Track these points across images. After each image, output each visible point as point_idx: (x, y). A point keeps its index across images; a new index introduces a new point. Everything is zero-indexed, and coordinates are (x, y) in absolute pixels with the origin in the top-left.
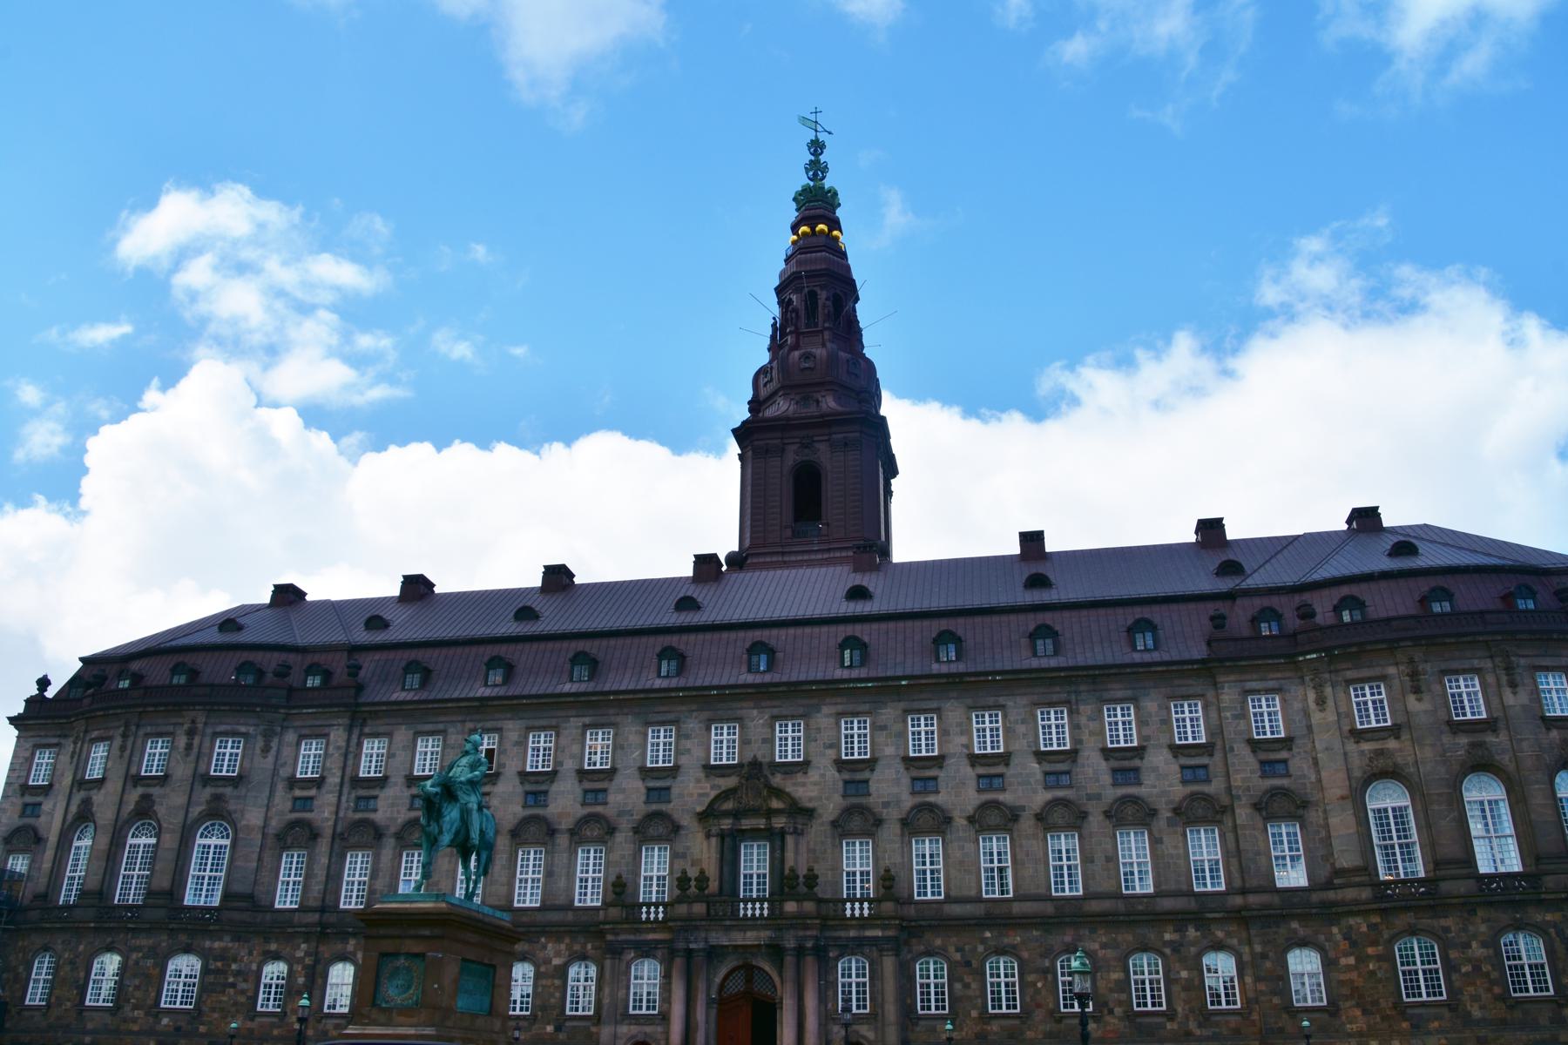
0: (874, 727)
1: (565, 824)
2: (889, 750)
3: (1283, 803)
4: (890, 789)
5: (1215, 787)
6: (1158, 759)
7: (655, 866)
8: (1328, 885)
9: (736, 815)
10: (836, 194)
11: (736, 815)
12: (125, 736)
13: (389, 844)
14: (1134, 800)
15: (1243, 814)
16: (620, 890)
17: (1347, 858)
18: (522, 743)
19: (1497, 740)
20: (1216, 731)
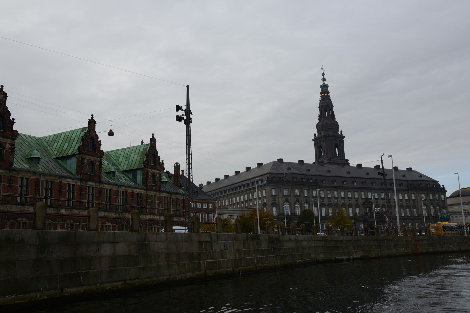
0: (378, 194)
1: (347, 205)
2: (380, 197)
3: (415, 207)
4: (380, 202)
5: (409, 204)
6: (404, 200)
7: (358, 210)
8: (419, 216)
9: (367, 205)
10: (328, 86)
11: (367, 205)
12: (292, 189)
13: (327, 207)
14: (402, 205)
15: (411, 207)
16: (355, 214)
17: (420, 213)
18: (340, 193)
19: (433, 202)
20: (408, 197)
